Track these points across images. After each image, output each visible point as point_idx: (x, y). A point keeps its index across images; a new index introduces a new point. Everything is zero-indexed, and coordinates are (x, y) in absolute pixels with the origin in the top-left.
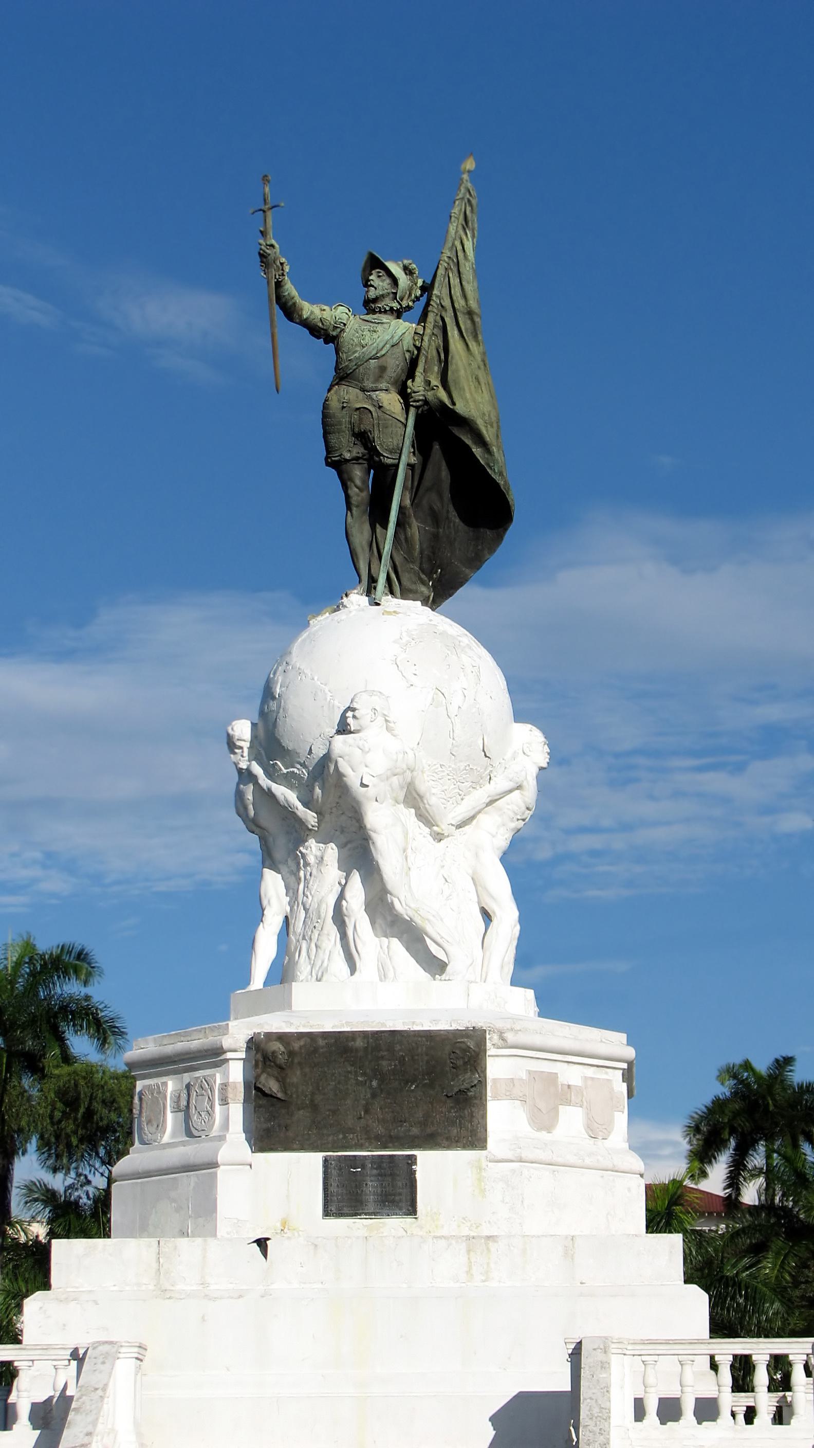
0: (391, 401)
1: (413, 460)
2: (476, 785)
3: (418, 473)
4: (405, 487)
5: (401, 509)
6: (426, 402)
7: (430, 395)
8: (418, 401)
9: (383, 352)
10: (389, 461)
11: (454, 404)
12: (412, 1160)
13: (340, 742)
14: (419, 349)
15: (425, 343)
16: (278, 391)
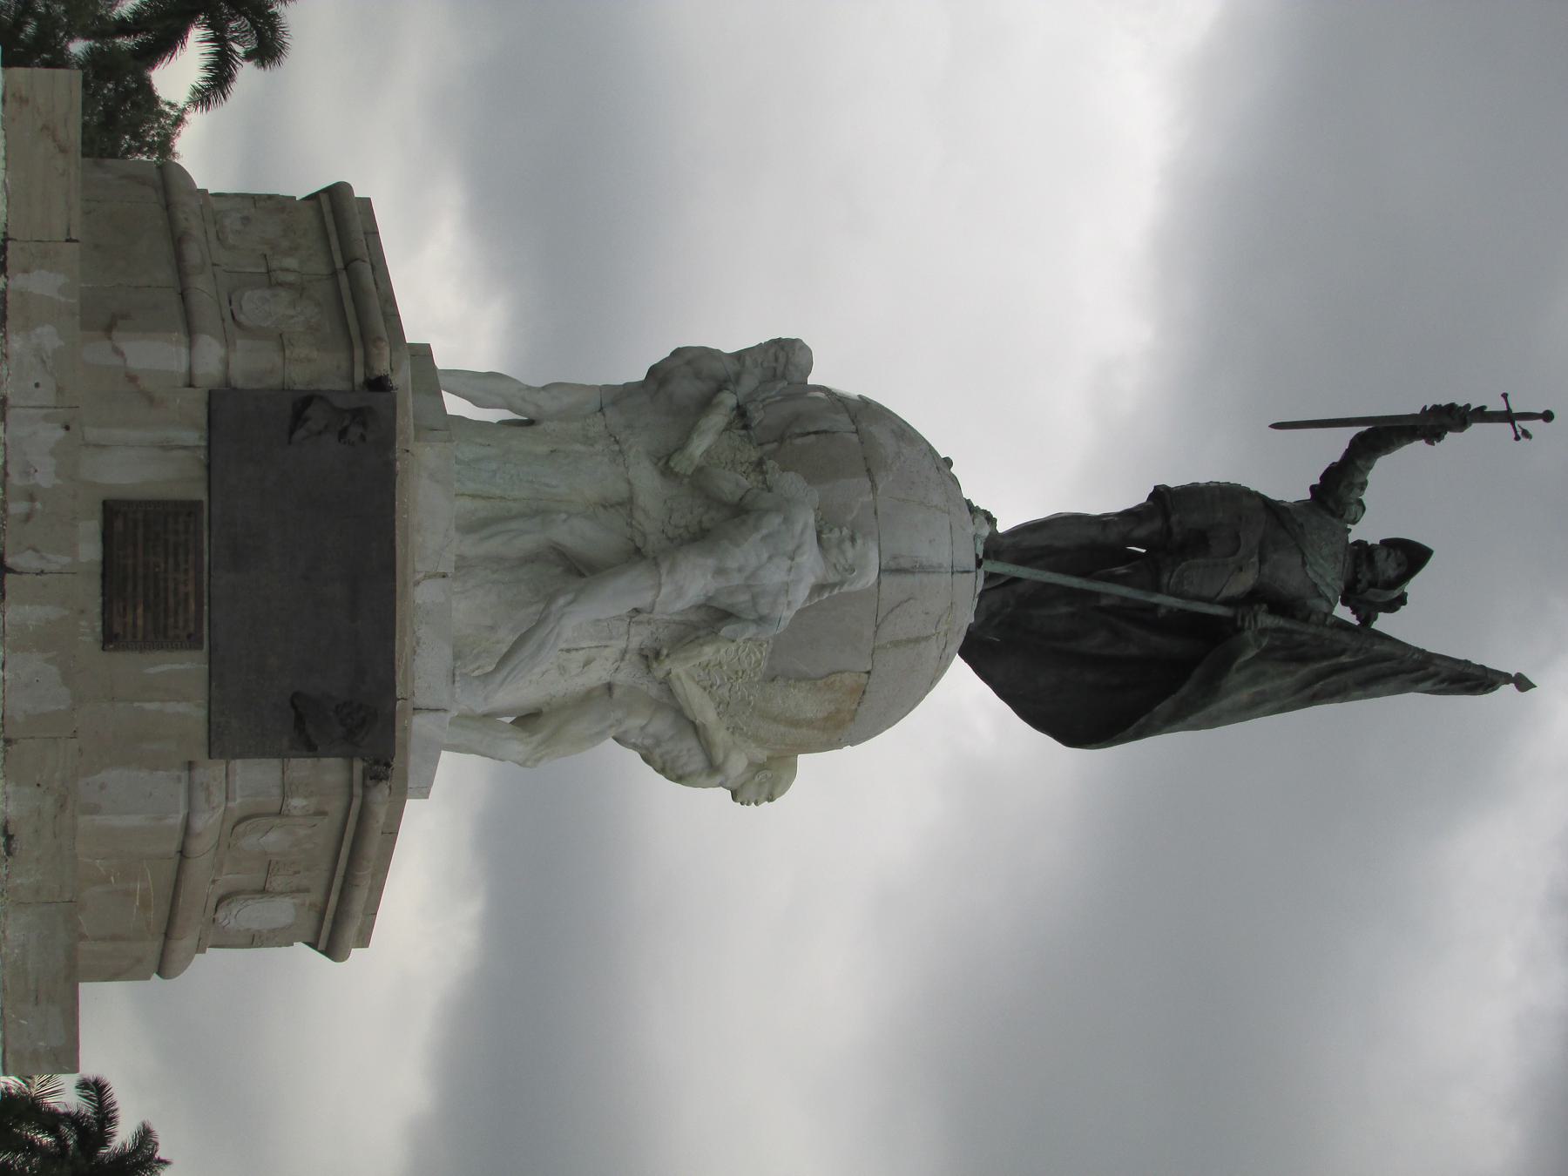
0: (1243, 582)
1: (1162, 611)
2: (723, 707)
3: (1143, 616)
4: (1124, 599)
5: (1097, 595)
6: (1240, 630)
7: (1248, 635)
8: (1243, 620)
9: (1311, 574)
10: (1165, 579)
11: (1239, 670)
12: (193, 641)
13: (806, 519)
14: (1306, 620)
15: (1312, 630)
16: (1276, 426)
